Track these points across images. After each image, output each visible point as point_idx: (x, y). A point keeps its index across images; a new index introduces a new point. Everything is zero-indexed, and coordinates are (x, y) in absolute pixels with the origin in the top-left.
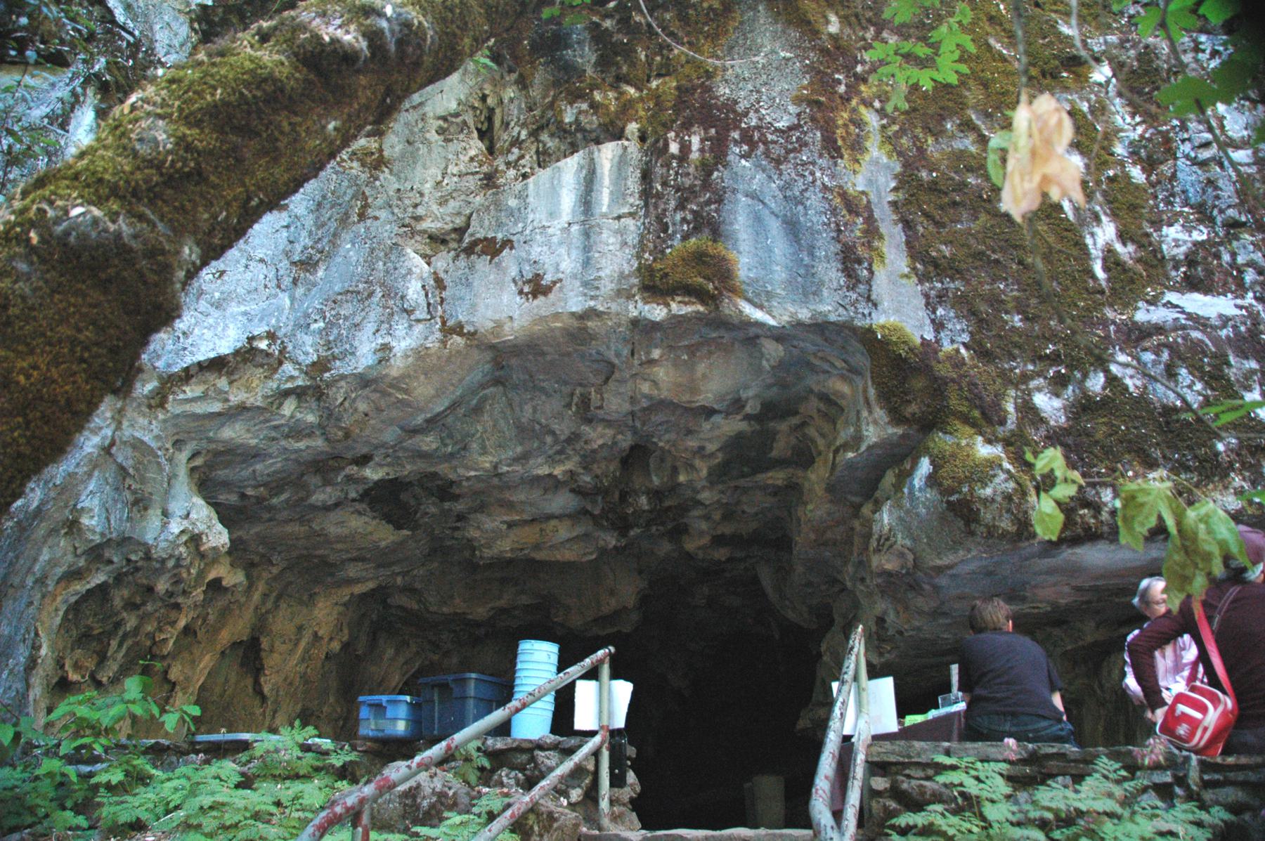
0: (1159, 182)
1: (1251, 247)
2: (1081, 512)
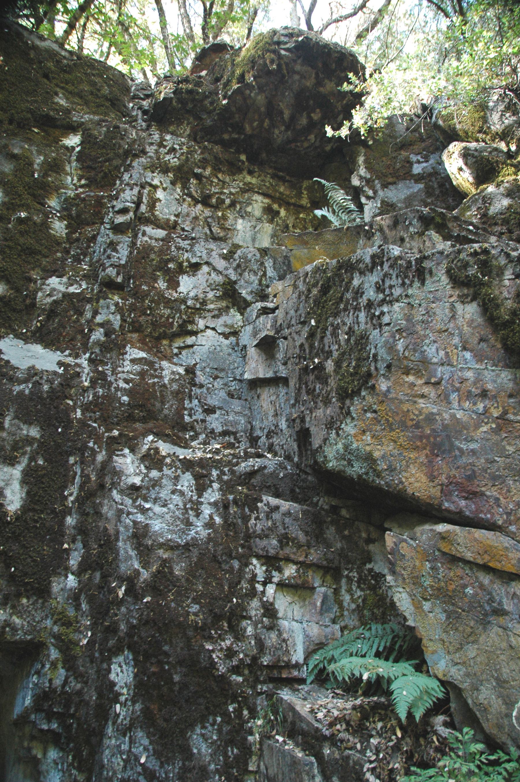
0: (78, 240)
1: (113, 308)
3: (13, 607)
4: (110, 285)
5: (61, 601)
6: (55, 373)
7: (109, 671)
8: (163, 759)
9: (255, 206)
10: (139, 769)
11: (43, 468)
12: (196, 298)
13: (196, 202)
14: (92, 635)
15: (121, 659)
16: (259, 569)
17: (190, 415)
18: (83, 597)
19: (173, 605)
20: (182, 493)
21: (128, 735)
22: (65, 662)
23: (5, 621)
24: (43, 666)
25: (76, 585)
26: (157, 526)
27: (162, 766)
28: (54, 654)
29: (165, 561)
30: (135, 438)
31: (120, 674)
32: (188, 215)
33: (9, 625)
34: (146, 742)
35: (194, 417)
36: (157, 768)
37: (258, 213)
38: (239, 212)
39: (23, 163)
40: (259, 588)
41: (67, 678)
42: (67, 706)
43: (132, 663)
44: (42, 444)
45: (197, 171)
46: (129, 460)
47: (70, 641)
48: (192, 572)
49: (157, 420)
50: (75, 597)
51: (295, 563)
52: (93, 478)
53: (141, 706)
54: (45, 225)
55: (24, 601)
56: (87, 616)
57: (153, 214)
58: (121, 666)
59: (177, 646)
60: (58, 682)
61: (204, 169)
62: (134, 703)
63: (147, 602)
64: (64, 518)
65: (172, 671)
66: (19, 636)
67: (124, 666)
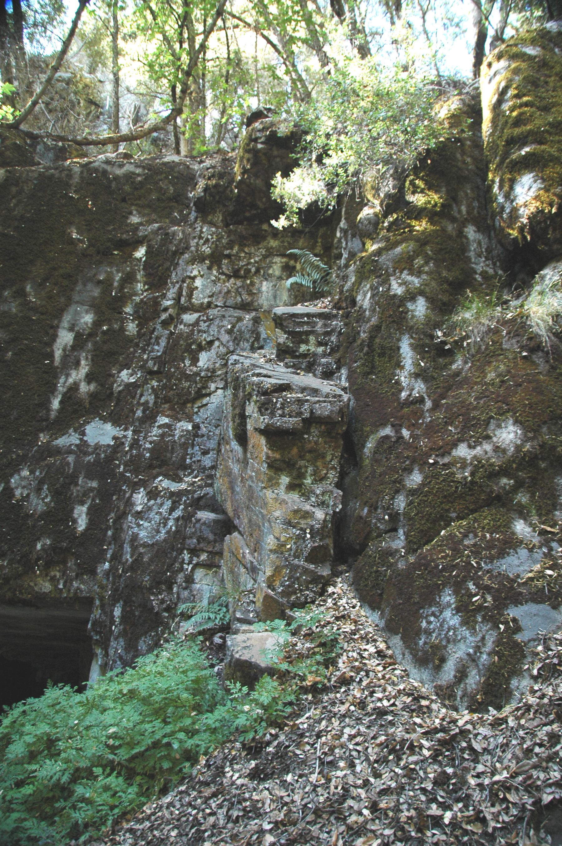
4: (151, 373)
6: (109, 445)
9: (275, 267)
11: (99, 504)
12: (208, 370)
13: (229, 277)
16: (186, 556)
17: (191, 459)
20: (161, 513)
26: (142, 534)
28: (97, 602)
29: (141, 553)
30: (148, 481)
32: (220, 292)
34: (122, 643)
35: (194, 459)
37: (277, 273)
38: (264, 275)
39: (107, 284)
40: (186, 566)
44: (98, 491)
45: (227, 252)
46: (140, 496)
48: (151, 560)
49: (168, 465)
50: (107, 573)
51: (207, 552)
52: (122, 508)
54: (122, 329)
57: (191, 303)
60: (98, 616)
61: (232, 249)
64: (107, 531)
66: (84, 594)
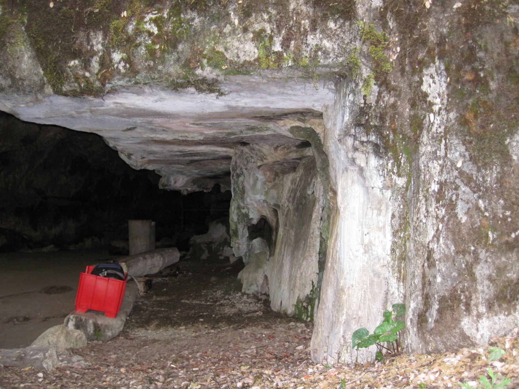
2: (72, 63)
3: (322, 32)
5: (368, 21)
7: (421, 83)
8: (480, 165)
10: (456, 173)
14: (401, 51)
15: (432, 70)
18: (389, 15)
19: (487, 8)
21: (444, 141)
22: (376, 78)
23: (317, 45)
24: (357, 85)
25: (381, 4)
27: (479, 170)
31: (433, 85)
33: (320, 49)
36: (474, 173)
41: (380, 93)
42: (382, 118)
43: (444, 73)
47: (379, 58)
53: (455, 115)
55: (331, 25)
56: (395, 33)
58: (432, 77)
59: (492, 52)
60: (372, 99)
62: (448, 111)
63: (457, 9)
65: (489, 79)
67: (436, 77)
